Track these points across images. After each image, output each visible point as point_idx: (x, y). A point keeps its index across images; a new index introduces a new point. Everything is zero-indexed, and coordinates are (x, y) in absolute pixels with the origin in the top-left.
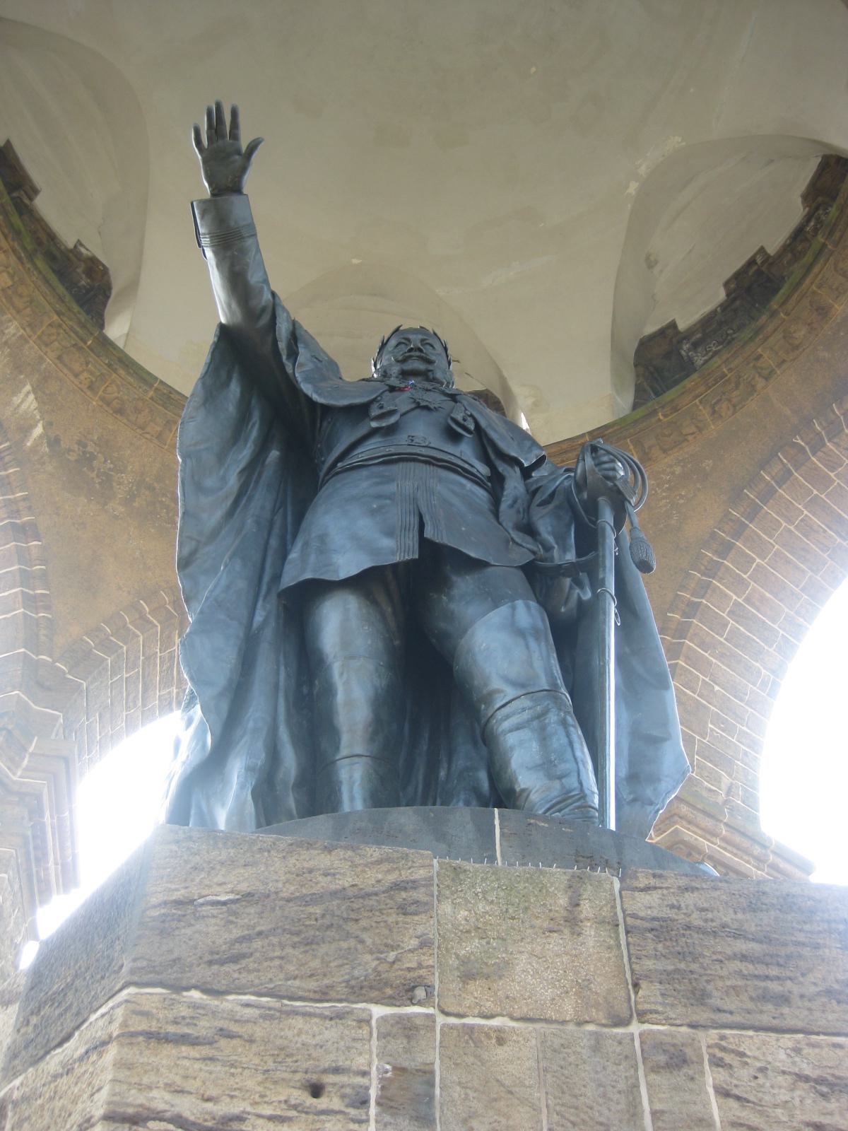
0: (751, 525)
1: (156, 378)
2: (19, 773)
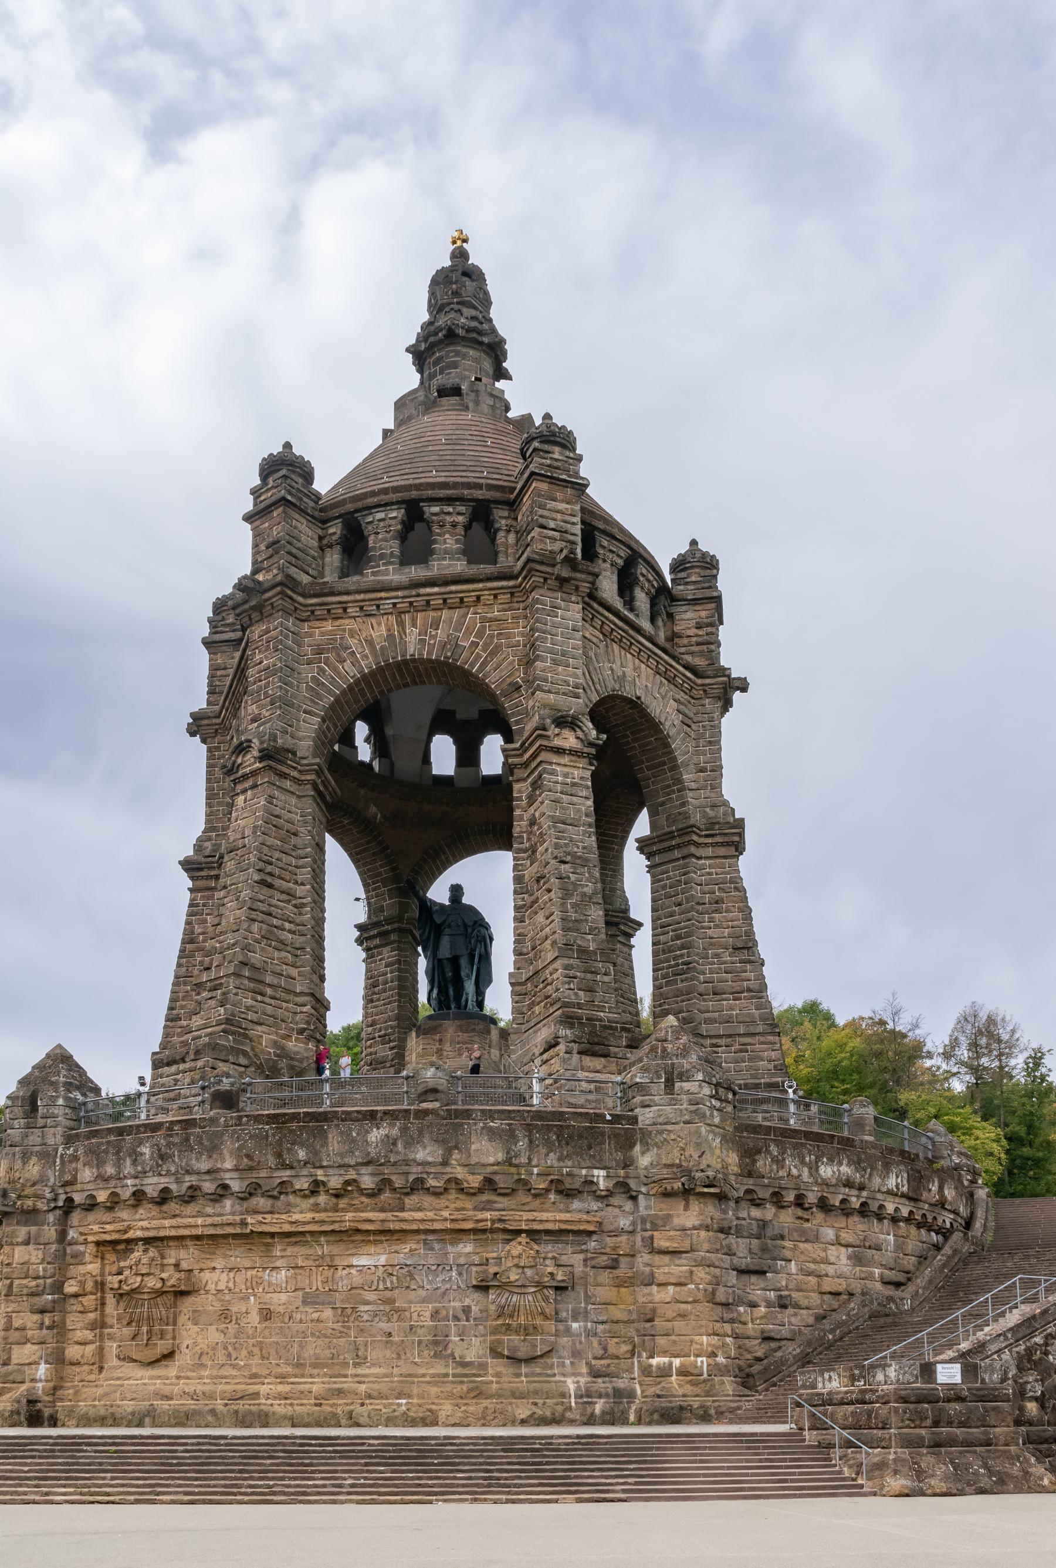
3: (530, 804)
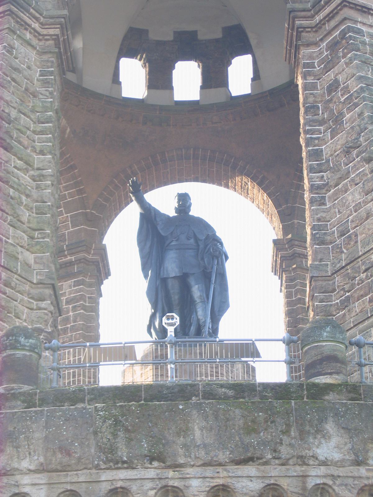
1: (104, 95)
2: (91, 255)
3: (327, 70)
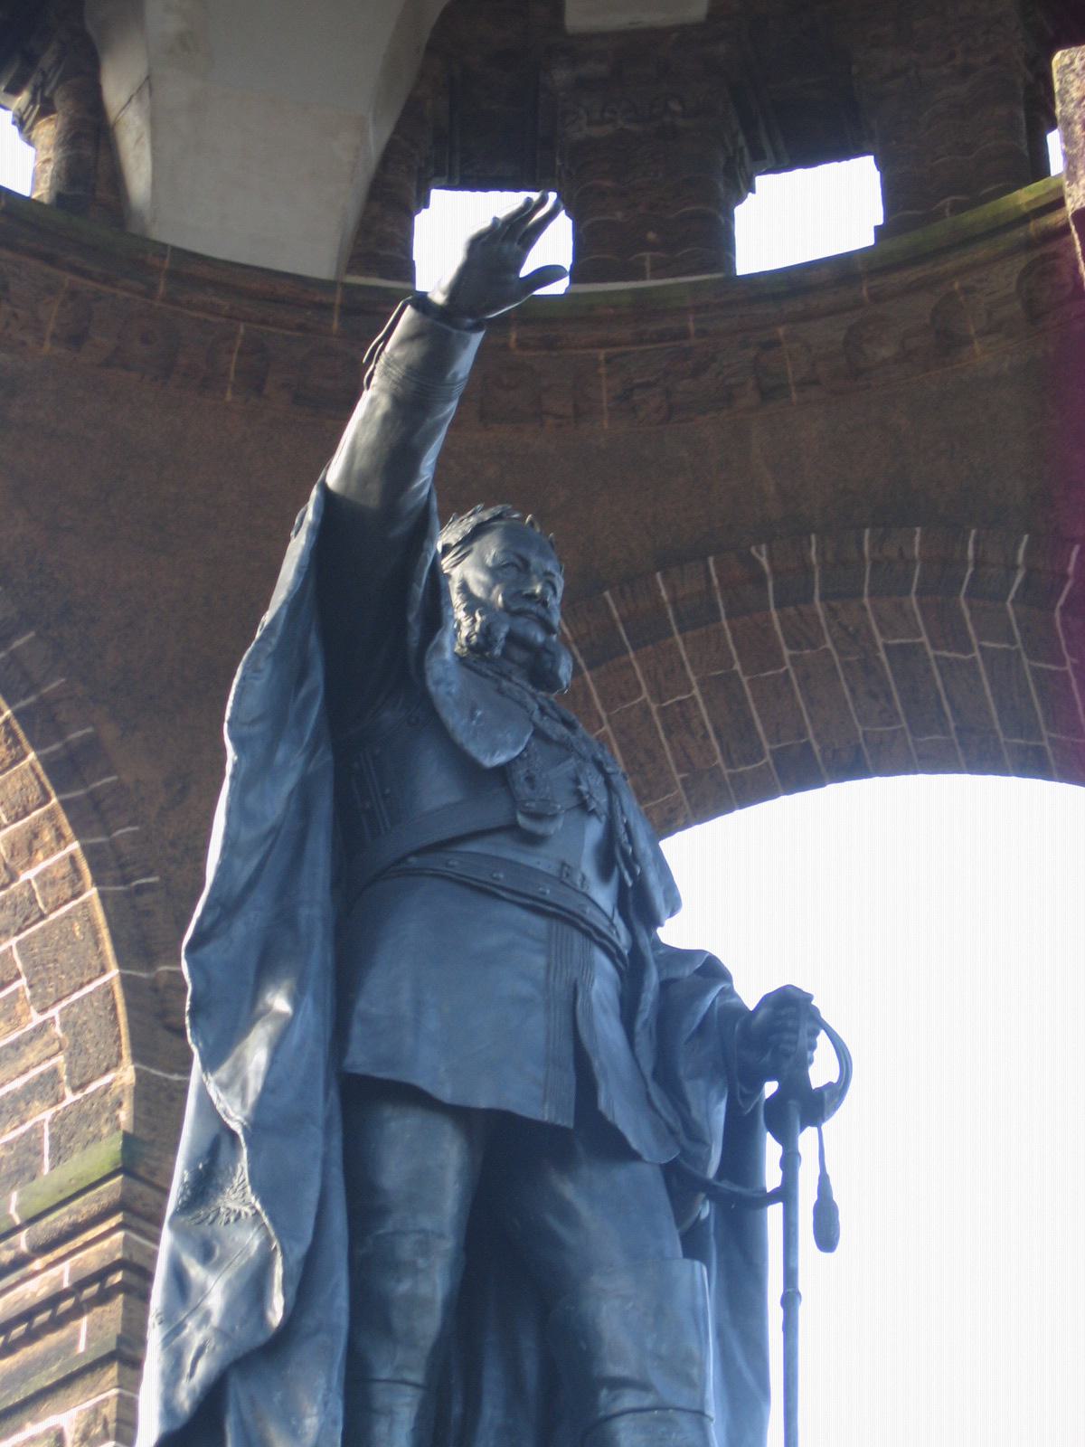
0: (587, 674)
